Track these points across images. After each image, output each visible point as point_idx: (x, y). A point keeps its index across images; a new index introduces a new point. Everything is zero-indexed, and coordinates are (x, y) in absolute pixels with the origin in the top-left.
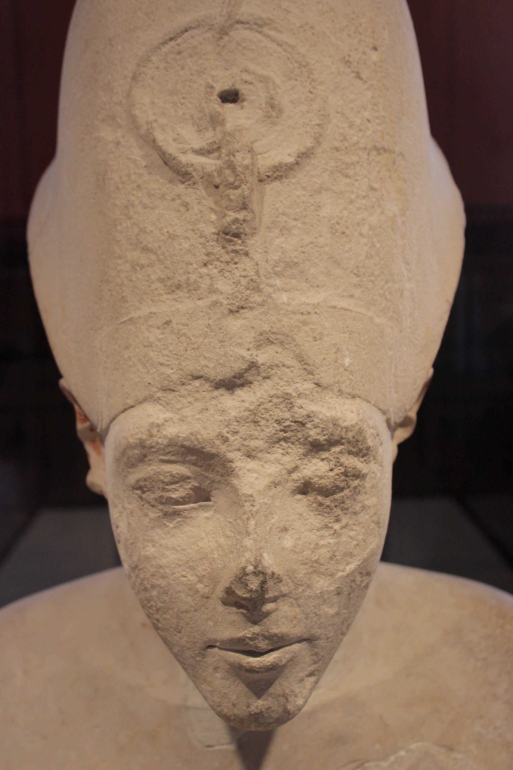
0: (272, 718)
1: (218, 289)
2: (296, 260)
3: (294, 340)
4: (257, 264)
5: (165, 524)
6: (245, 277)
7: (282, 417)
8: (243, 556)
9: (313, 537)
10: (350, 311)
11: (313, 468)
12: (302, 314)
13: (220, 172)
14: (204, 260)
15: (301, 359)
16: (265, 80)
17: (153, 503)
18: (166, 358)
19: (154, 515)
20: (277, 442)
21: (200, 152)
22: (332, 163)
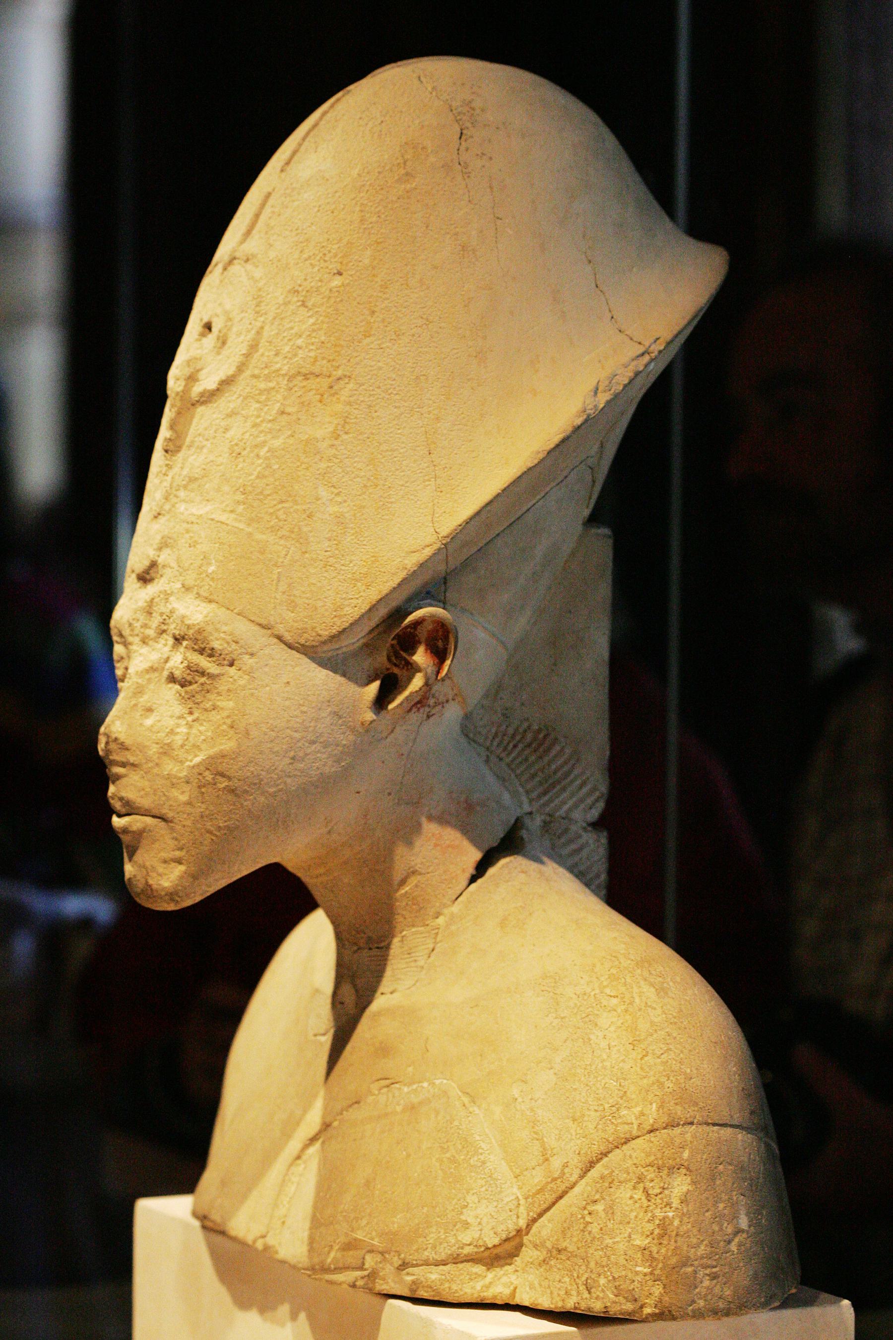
2: (197, 476)
9: (171, 723)
10: (227, 525)
22: (248, 389)
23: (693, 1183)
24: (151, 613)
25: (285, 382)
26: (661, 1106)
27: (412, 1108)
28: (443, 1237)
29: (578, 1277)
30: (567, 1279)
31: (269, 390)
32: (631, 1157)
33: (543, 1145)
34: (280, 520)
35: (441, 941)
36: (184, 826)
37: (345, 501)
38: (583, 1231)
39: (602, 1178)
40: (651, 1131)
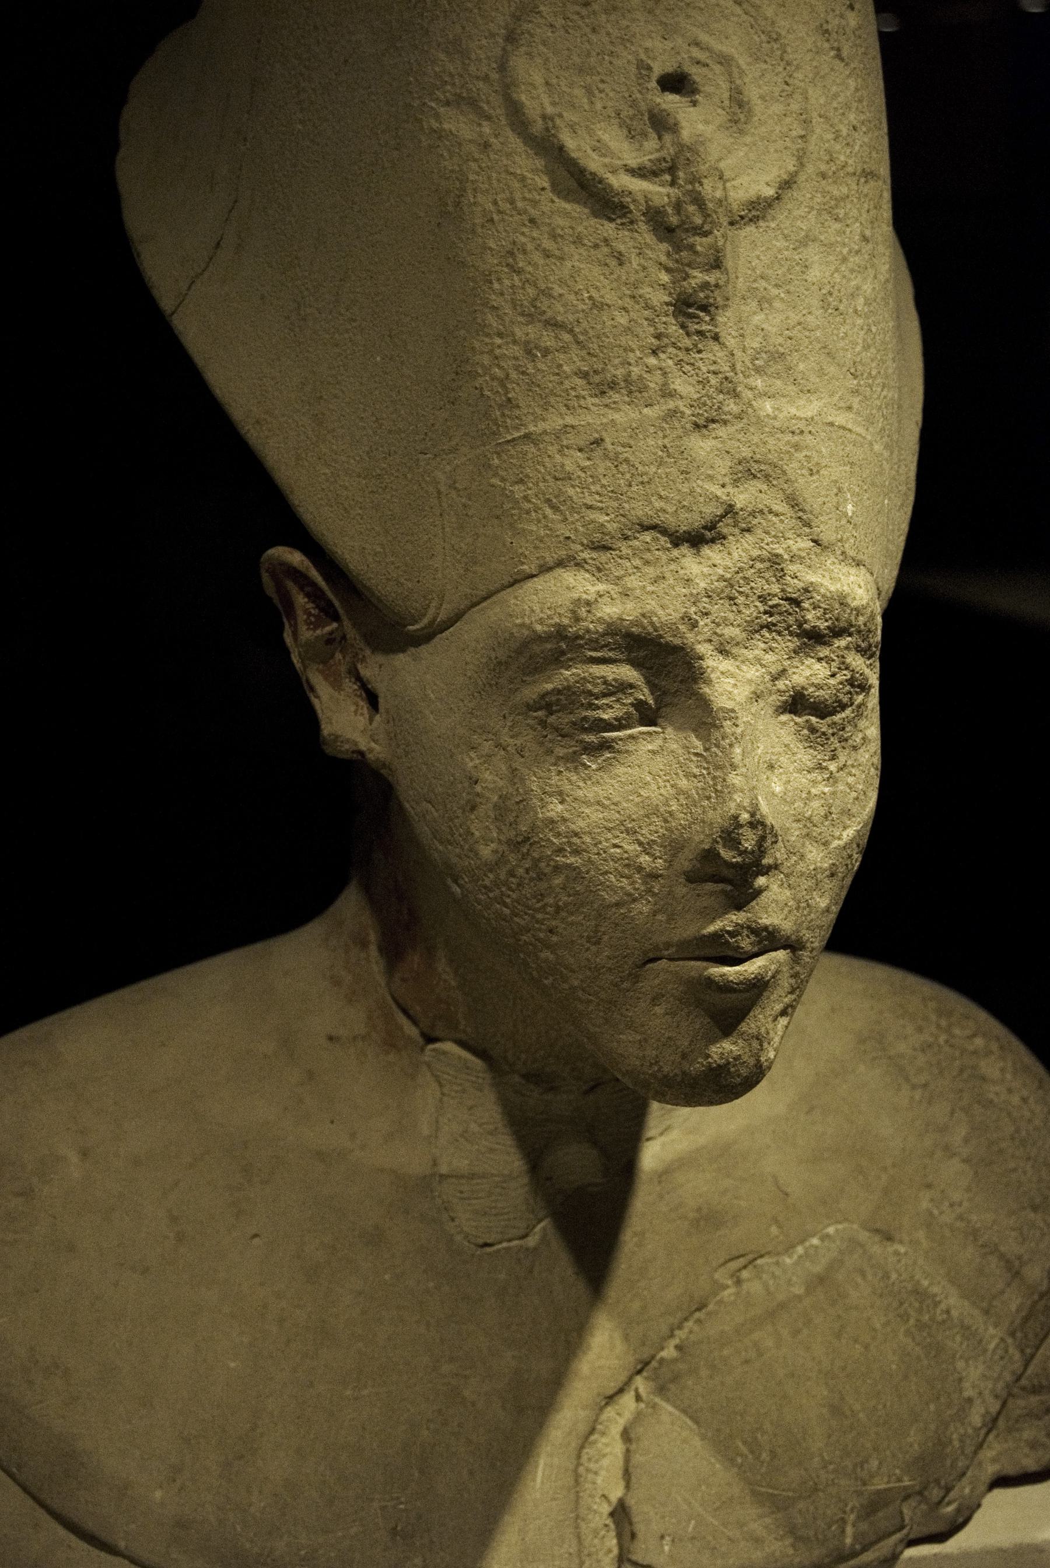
0: (739, 1076)
1: (675, 390)
2: (781, 350)
3: (784, 472)
4: (733, 355)
5: (584, 765)
6: (715, 373)
7: (767, 591)
8: (731, 799)
10: (850, 430)
11: (808, 673)
12: (793, 433)
13: (678, 206)
14: (652, 344)
15: (793, 502)
16: (725, 61)
17: (567, 729)
18: (597, 497)
19: (566, 751)
20: (757, 632)
21: (639, 172)
22: (819, 198)
33: (1002, 1256)
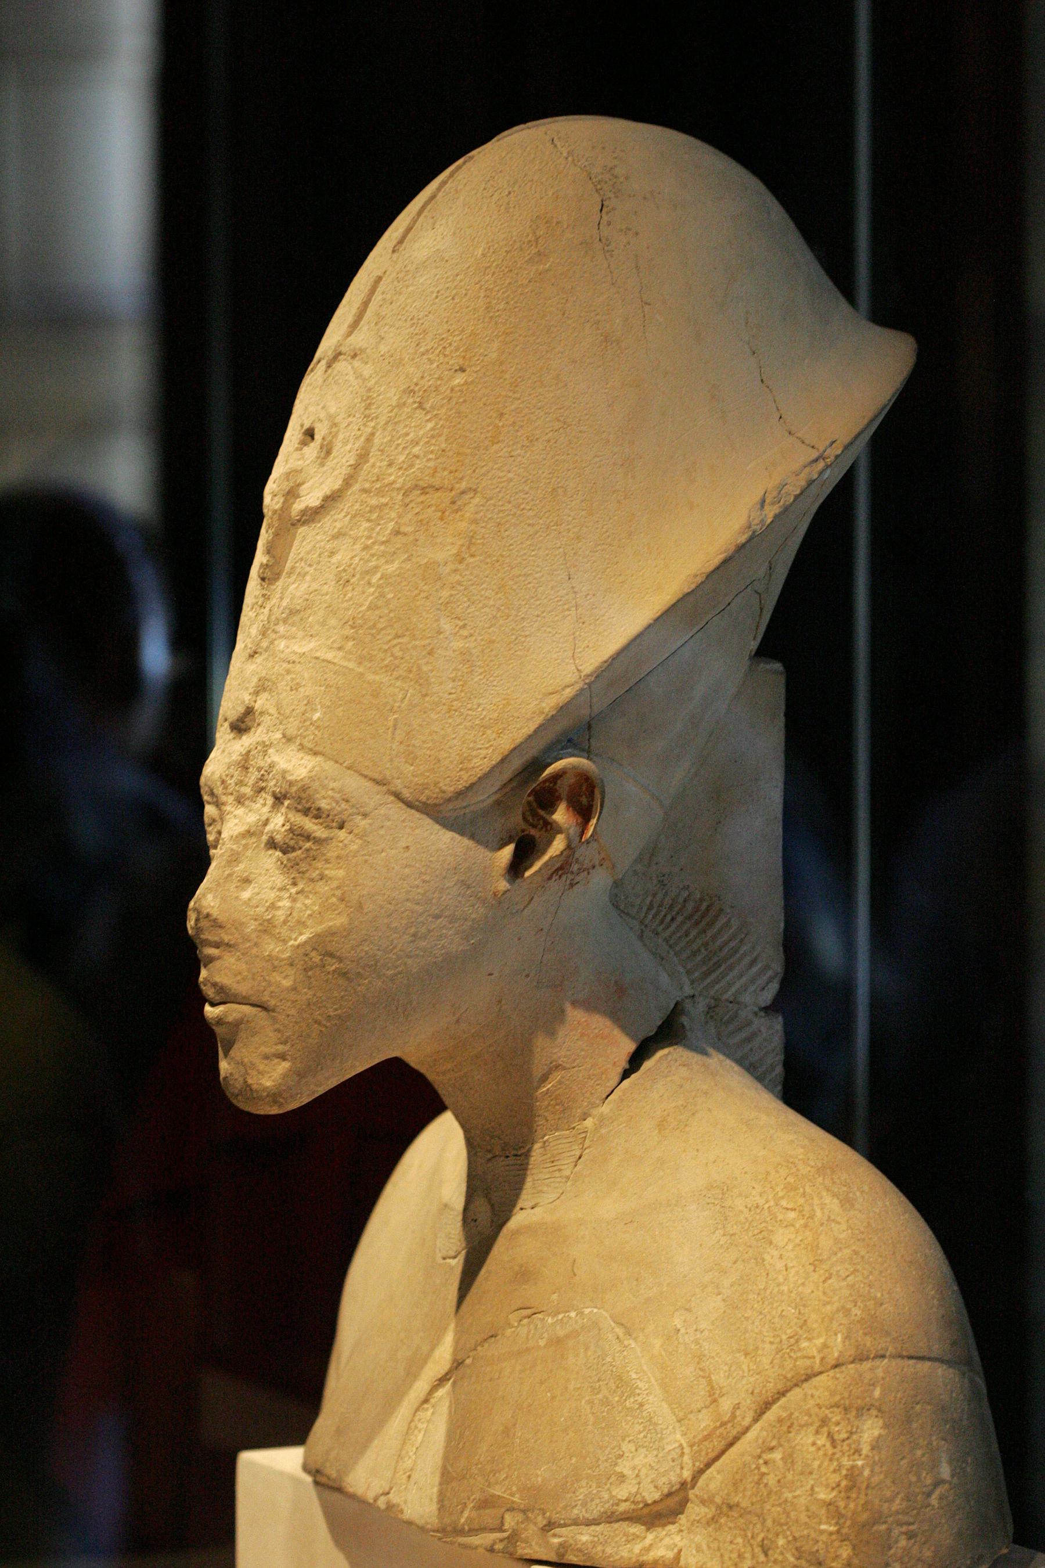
2: (298, 607)
9: (273, 895)
10: (334, 664)
22: (357, 506)
23: (886, 1426)
24: (247, 768)
25: (400, 497)
26: (847, 1337)
27: (557, 1342)
28: (595, 1492)
29: (753, 1537)
30: (739, 1540)
31: (381, 507)
32: (812, 1396)
33: (710, 1382)
34: (396, 658)
35: (589, 1147)
36: (288, 1016)
37: (471, 635)
38: (758, 1483)
39: (780, 1421)
40: (836, 1366)
